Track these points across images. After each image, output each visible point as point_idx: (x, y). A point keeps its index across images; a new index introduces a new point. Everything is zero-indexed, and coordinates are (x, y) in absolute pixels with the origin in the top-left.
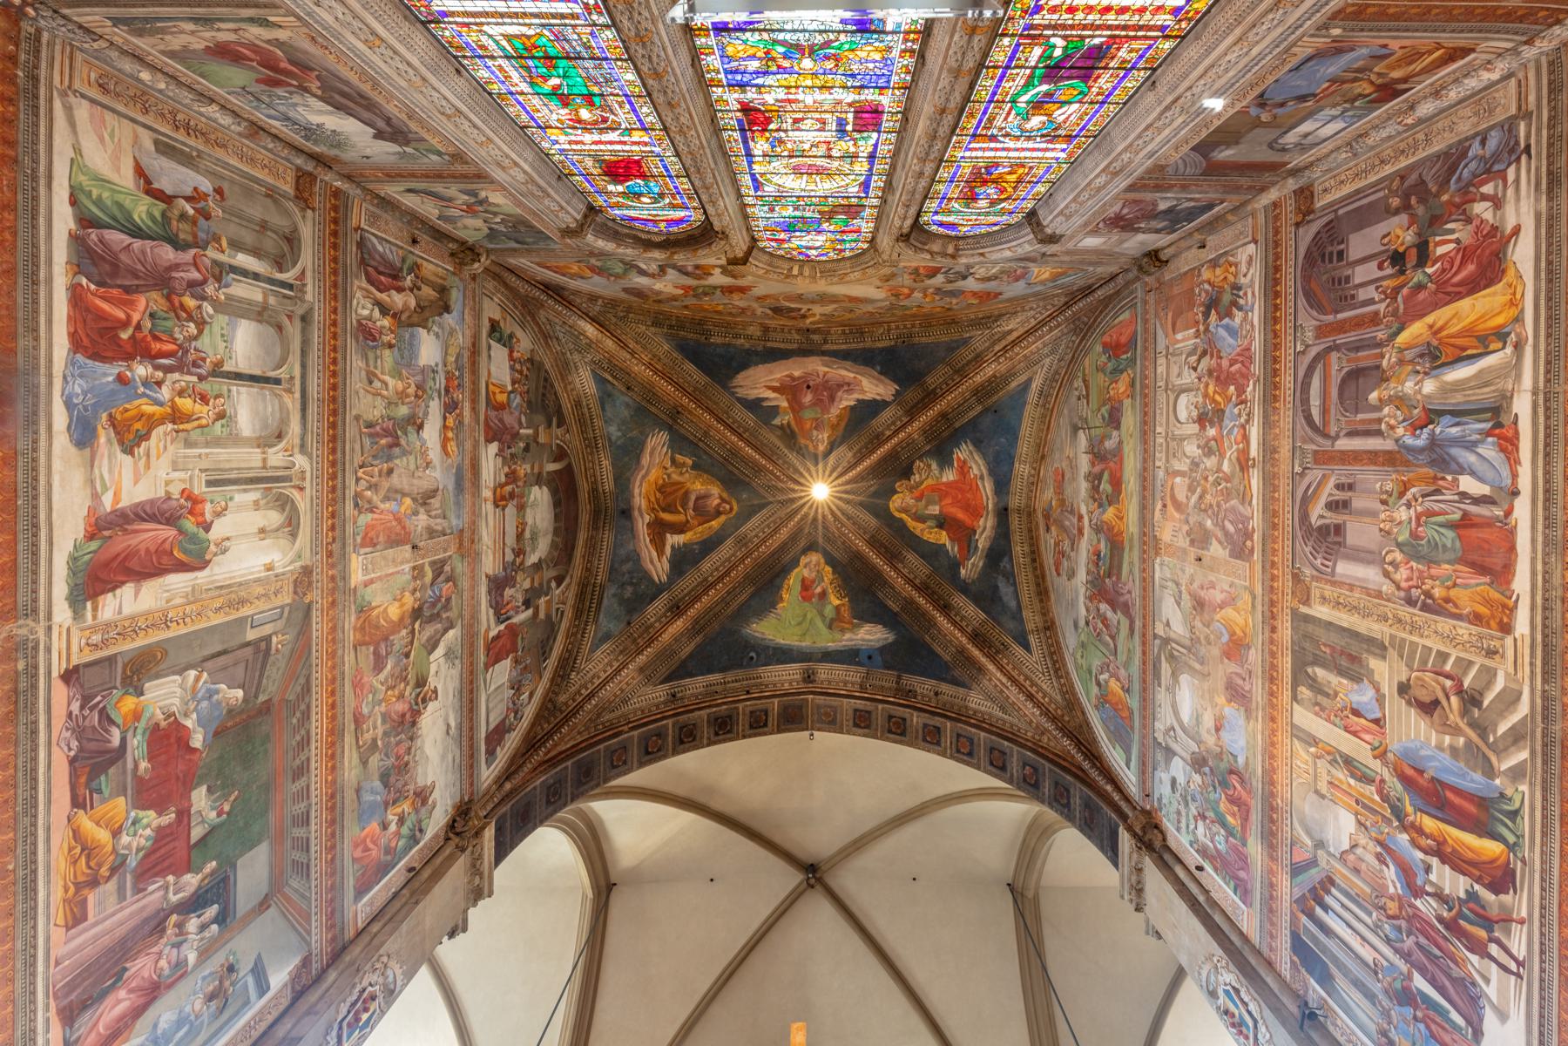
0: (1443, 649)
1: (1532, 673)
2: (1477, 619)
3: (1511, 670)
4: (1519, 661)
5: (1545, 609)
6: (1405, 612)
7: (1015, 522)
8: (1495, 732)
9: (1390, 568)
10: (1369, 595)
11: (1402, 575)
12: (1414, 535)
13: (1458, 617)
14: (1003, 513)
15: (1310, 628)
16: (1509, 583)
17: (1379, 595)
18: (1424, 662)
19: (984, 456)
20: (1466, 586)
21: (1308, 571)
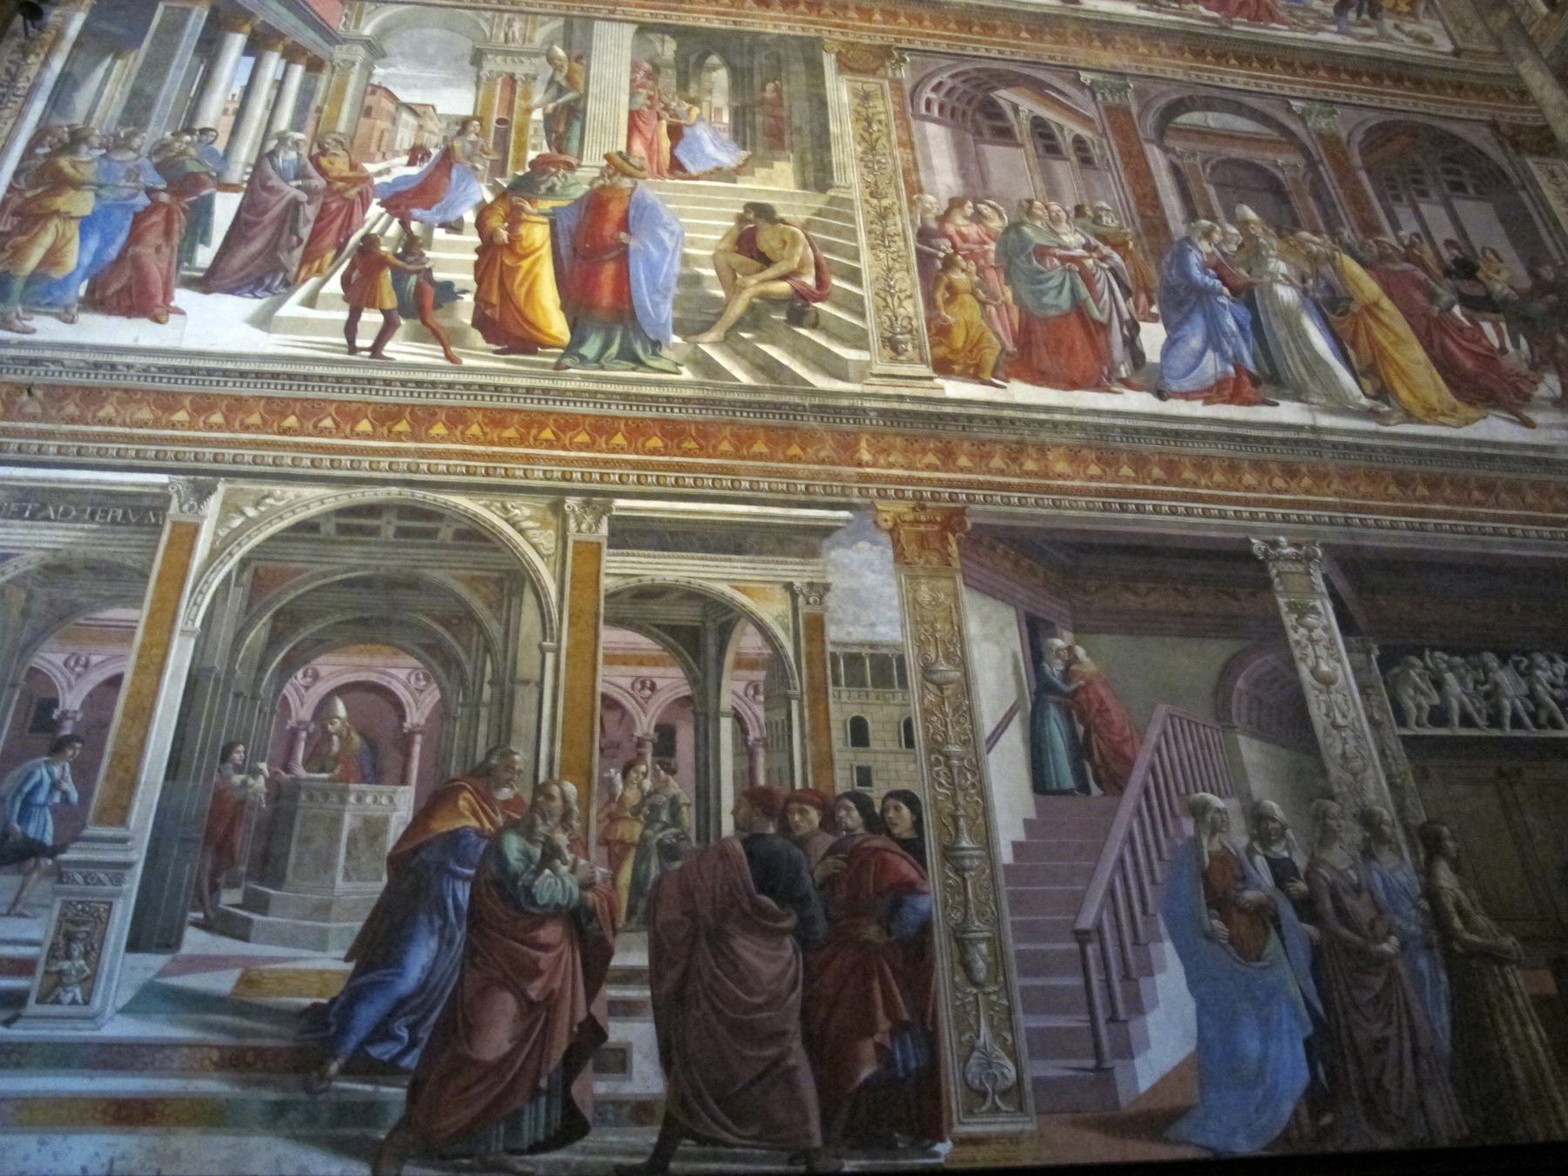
0: (866, 277)
1: (887, 397)
2: (940, 331)
3: (877, 369)
4: (900, 382)
5: (998, 420)
6: (902, 225)
8: (763, 342)
9: (969, 208)
10: (906, 172)
11: (961, 223)
12: (1042, 252)
13: (930, 302)
16: (1020, 376)
17: (915, 189)
18: (829, 247)
20: (987, 317)
21: (903, 73)
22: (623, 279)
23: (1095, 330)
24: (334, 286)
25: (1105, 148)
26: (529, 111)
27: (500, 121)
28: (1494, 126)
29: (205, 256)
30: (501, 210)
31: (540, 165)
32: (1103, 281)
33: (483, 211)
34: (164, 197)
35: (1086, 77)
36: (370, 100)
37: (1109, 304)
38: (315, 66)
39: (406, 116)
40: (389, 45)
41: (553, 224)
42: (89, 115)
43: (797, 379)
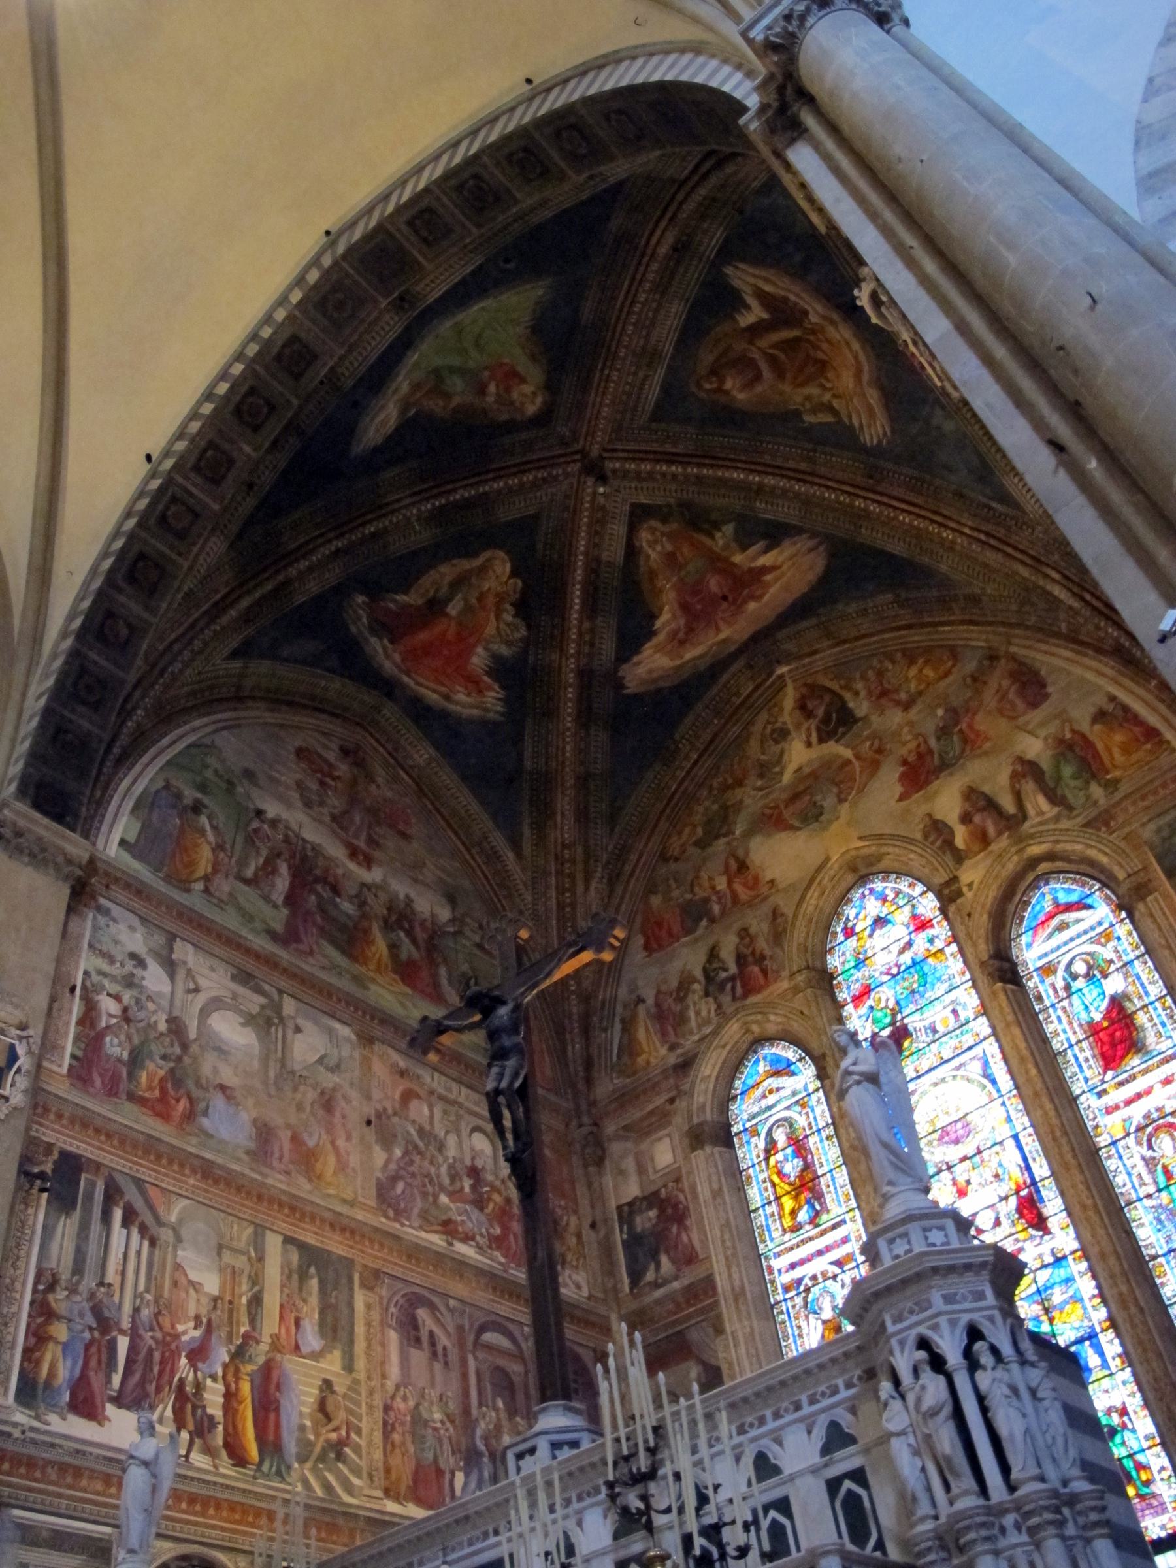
0: (364, 1432)
2: (388, 1471)
3: (367, 1492)
6: (378, 1401)
7: (369, 697)
13: (385, 1454)
14: (388, 687)
15: (344, 1281)
17: (384, 1376)
19: (471, 721)
21: (384, 1292)
22: (278, 1426)
23: (440, 1472)
24: (169, 1413)
25: (454, 1356)
26: (240, 1296)
27: (231, 1302)
28: (594, 1350)
29: (116, 1379)
30: (231, 1370)
31: (246, 1336)
32: (446, 1443)
33: (226, 1366)
34: (96, 1334)
35: (452, 1303)
36: (177, 1274)
37: (448, 1460)
38: (153, 1243)
39: (192, 1291)
40: (184, 1232)
41: (252, 1382)
42: (58, 1265)
43: (339, 1497)
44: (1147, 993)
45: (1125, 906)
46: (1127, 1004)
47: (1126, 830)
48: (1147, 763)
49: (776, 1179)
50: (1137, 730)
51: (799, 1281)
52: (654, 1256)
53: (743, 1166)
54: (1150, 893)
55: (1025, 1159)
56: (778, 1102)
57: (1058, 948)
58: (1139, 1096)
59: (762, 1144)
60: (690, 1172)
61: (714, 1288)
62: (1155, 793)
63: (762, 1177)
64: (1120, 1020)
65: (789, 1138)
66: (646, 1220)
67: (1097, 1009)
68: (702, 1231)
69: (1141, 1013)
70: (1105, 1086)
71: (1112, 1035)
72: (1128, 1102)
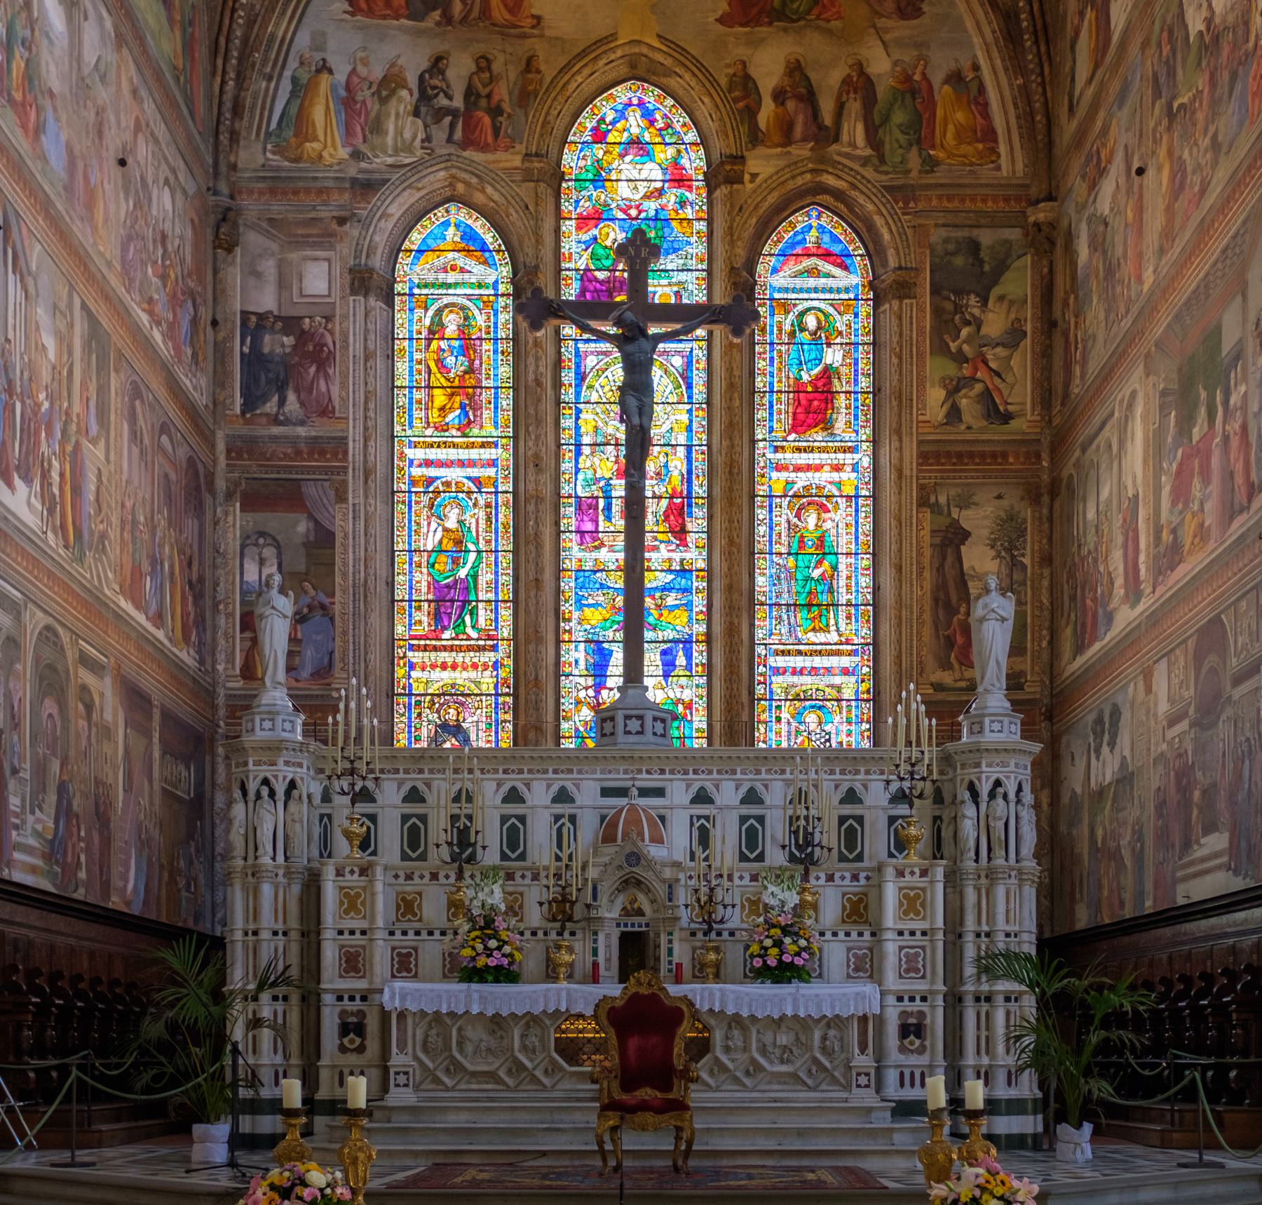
44: (856, 380)
45: (879, 293)
46: (836, 381)
47: (920, 221)
48: (972, 164)
49: (432, 365)
50: (980, 120)
51: (430, 481)
52: (281, 390)
53: (401, 333)
54: (910, 298)
55: (690, 472)
56: (456, 285)
57: (801, 290)
58: (808, 468)
59: (427, 322)
60: (345, 317)
61: (346, 452)
62: (963, 201)
63: (417, 356)
64: (823, 392)
65: (461, 332)
66: (278, 344)
67: (809, 370)
68: (344, 385)
69: (843, 396)
70: (784, 444)
71: (811, 401)
72: (798, 469)
